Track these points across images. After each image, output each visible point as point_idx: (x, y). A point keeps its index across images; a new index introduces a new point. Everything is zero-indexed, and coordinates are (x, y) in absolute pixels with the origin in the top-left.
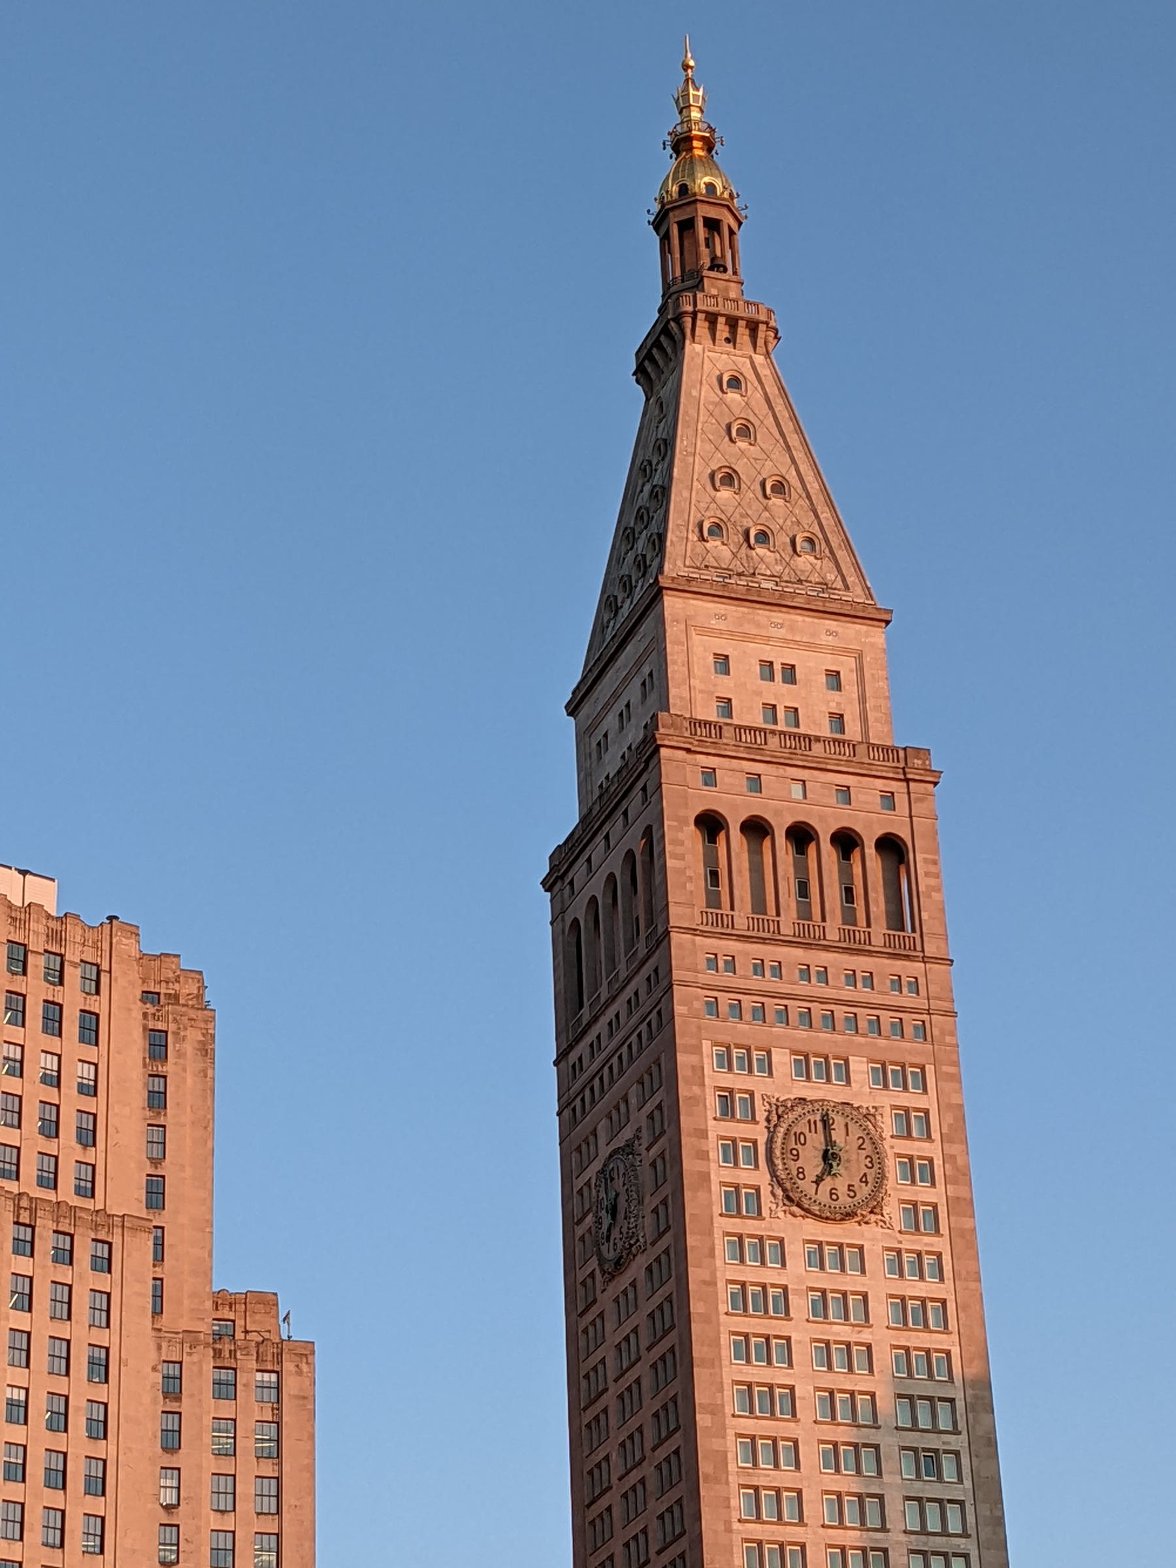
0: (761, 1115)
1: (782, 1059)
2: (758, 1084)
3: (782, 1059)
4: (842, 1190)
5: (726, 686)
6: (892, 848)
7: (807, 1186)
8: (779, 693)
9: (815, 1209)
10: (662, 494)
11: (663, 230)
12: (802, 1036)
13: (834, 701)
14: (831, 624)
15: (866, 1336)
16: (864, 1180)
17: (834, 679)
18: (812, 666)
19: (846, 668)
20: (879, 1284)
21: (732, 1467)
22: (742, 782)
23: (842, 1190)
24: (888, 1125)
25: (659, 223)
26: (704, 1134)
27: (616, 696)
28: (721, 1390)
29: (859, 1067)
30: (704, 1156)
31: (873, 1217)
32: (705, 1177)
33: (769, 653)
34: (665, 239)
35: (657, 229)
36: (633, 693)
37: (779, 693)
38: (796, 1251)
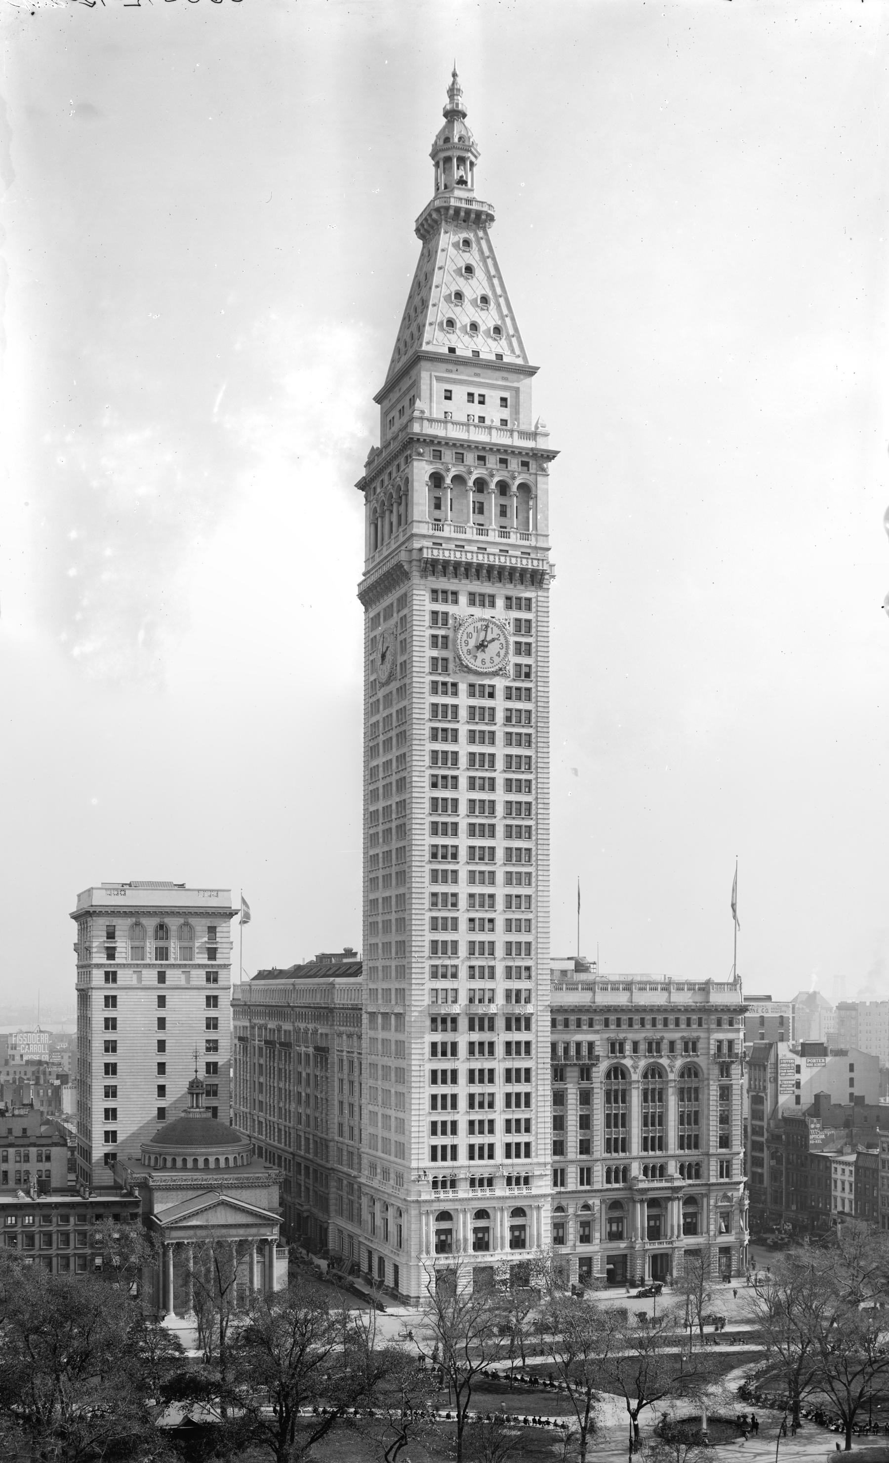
2: (450, 609)
4: (488, 661)
6: (525, 488)
10: (424, 303)
11: (437, 159)
15: (492, 728)
16: (498, 655)
17: (504, 400)
23: (488, 661)
24: (511, 629)
25: (433, 155)
27: (398, 401)
33: (471, 390)
34: (437, 165)
35: (433, 159)
36: (406, 403)
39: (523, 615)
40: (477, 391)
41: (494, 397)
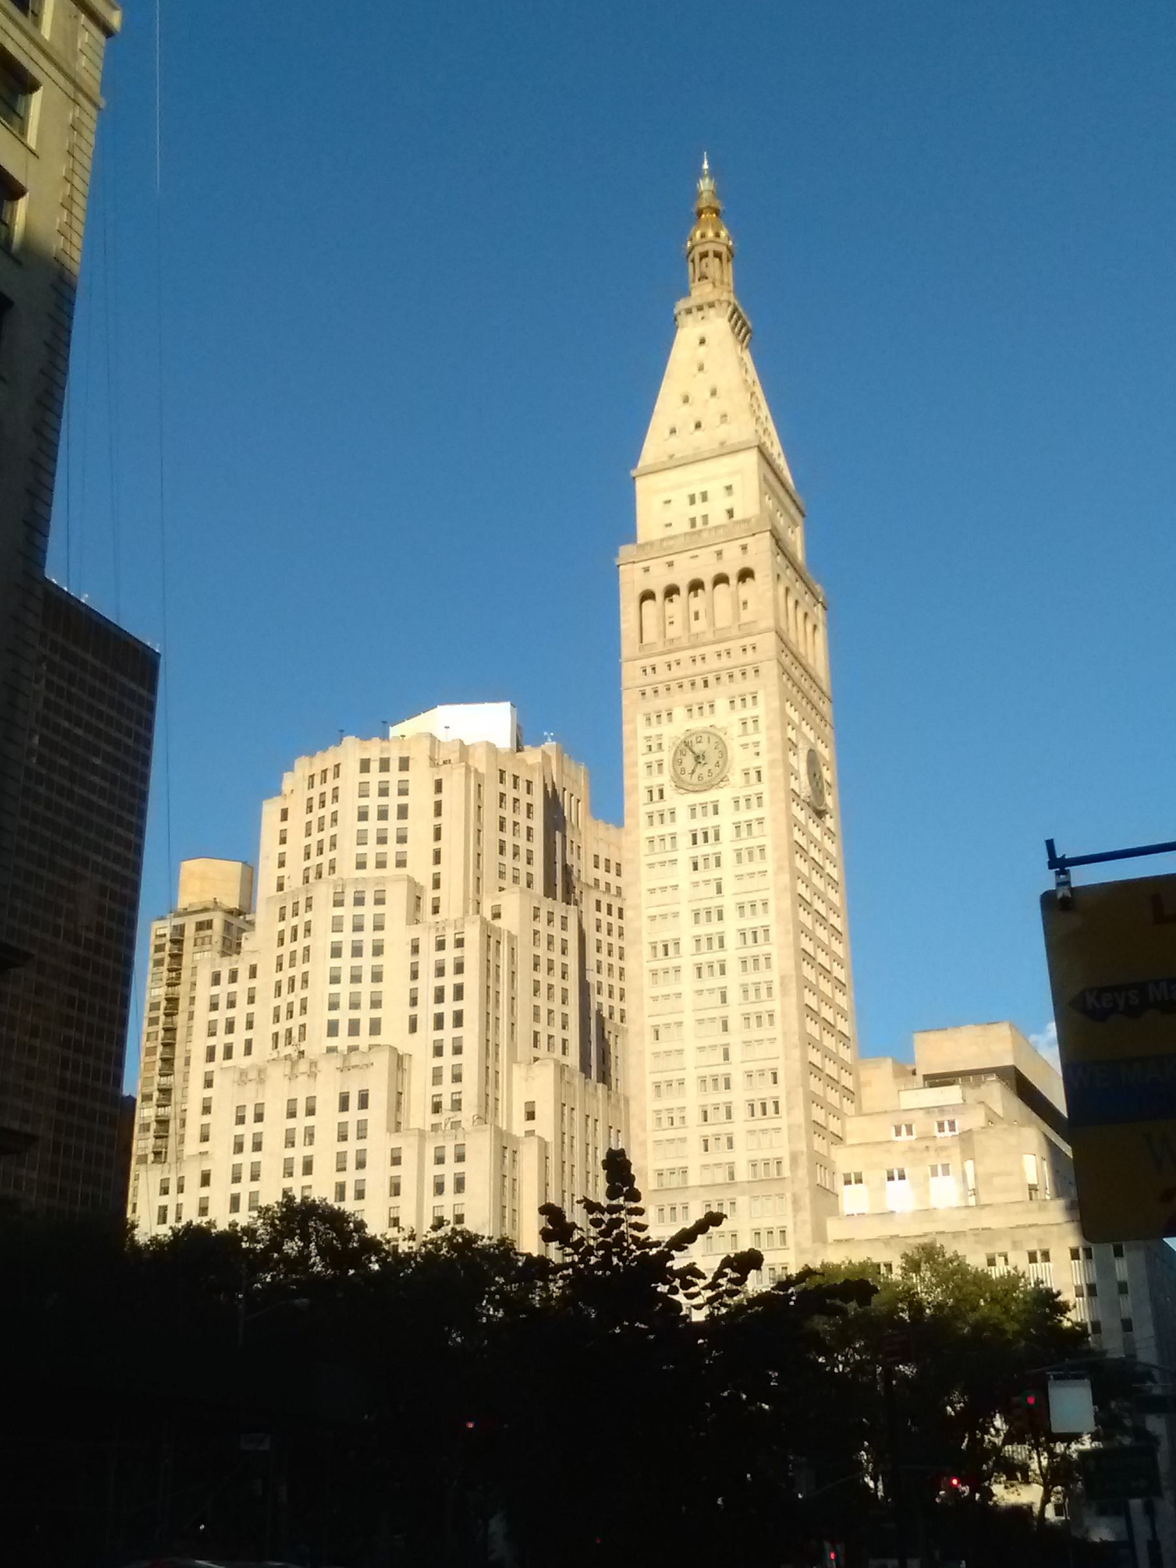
0: (665, 746)
1: (679, 713)
3: (679, 713)
7: (686, 777)
8: (699, 510)
9: (690, 788)
13: (728, 503)
14: (726, 460)
18: (715, 489)
19: (735, 482)
20: (725, 821)
21: (644, 934)
22: (664, 569)
24: (737, 729)
26: (636, 764)
28: (640, 895)
29: (722, 704)
30: (635, 776)
31: (722, 784)
32: (636, 787)
37: (699, 510)
39: (749, 712)
40: (697, 491)
41: (715, 489)
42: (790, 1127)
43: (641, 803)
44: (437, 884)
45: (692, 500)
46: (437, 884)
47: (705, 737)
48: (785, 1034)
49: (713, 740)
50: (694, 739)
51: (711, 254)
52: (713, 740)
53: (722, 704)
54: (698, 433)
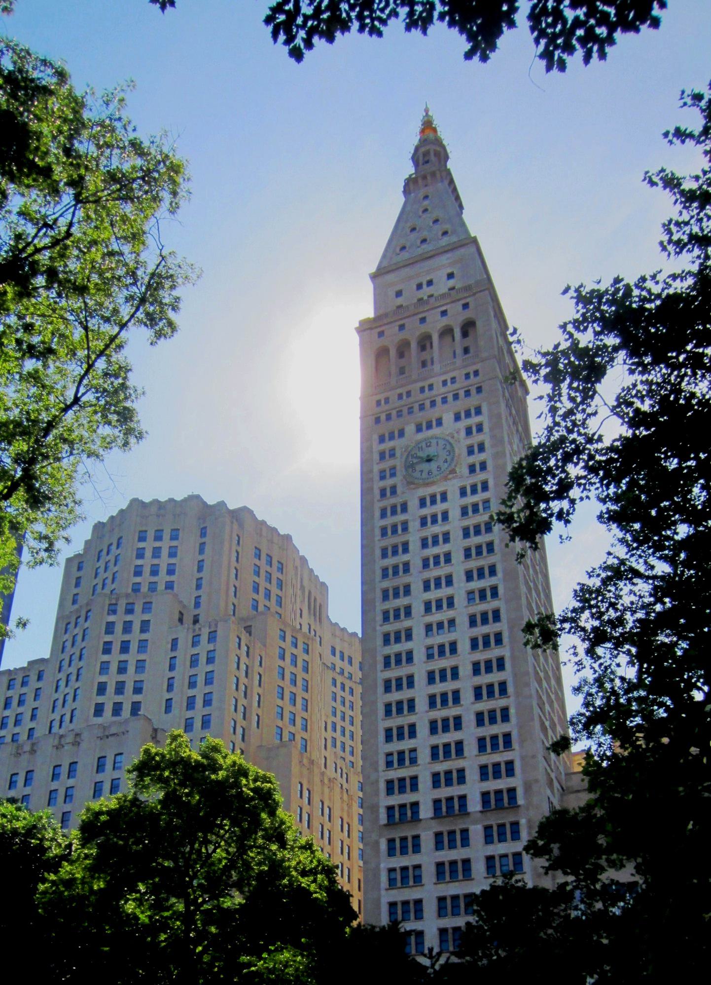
0: (398, 454)
1: (410, 429)
3: (410, 429)
5: (400, 301)
12: (421, 417)
16: (446, 461)
21: (377, 604)
29: (448, 418)
31: (451, 476)
37: (426, 291)
38: (413, 504)
42: (523, 758)
43: (375, 500)
44: (197, 605)
45: (419, 286)
46: (197, 605)
47: (434, 442)
48: (515, 675)
49: (441, 442)
50: (424, 445)
51: (432, 153)
52: (441, 442)
53: (448, 418)
54: (424, 246)
